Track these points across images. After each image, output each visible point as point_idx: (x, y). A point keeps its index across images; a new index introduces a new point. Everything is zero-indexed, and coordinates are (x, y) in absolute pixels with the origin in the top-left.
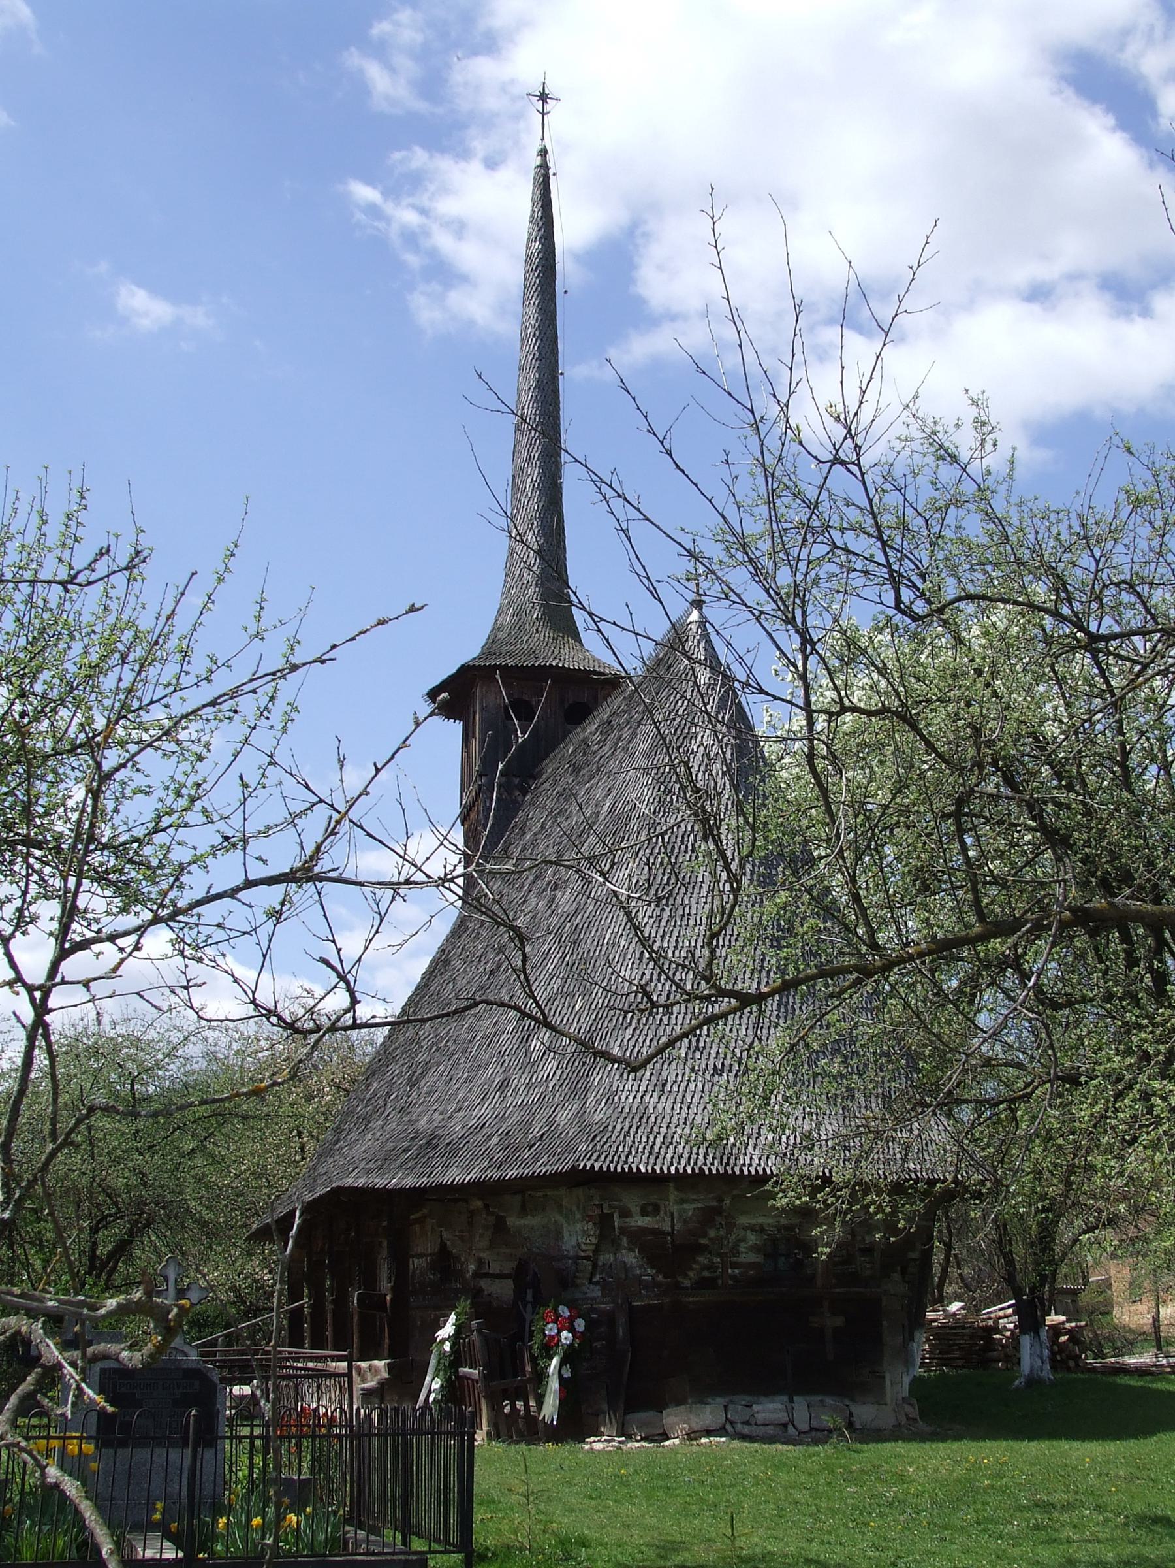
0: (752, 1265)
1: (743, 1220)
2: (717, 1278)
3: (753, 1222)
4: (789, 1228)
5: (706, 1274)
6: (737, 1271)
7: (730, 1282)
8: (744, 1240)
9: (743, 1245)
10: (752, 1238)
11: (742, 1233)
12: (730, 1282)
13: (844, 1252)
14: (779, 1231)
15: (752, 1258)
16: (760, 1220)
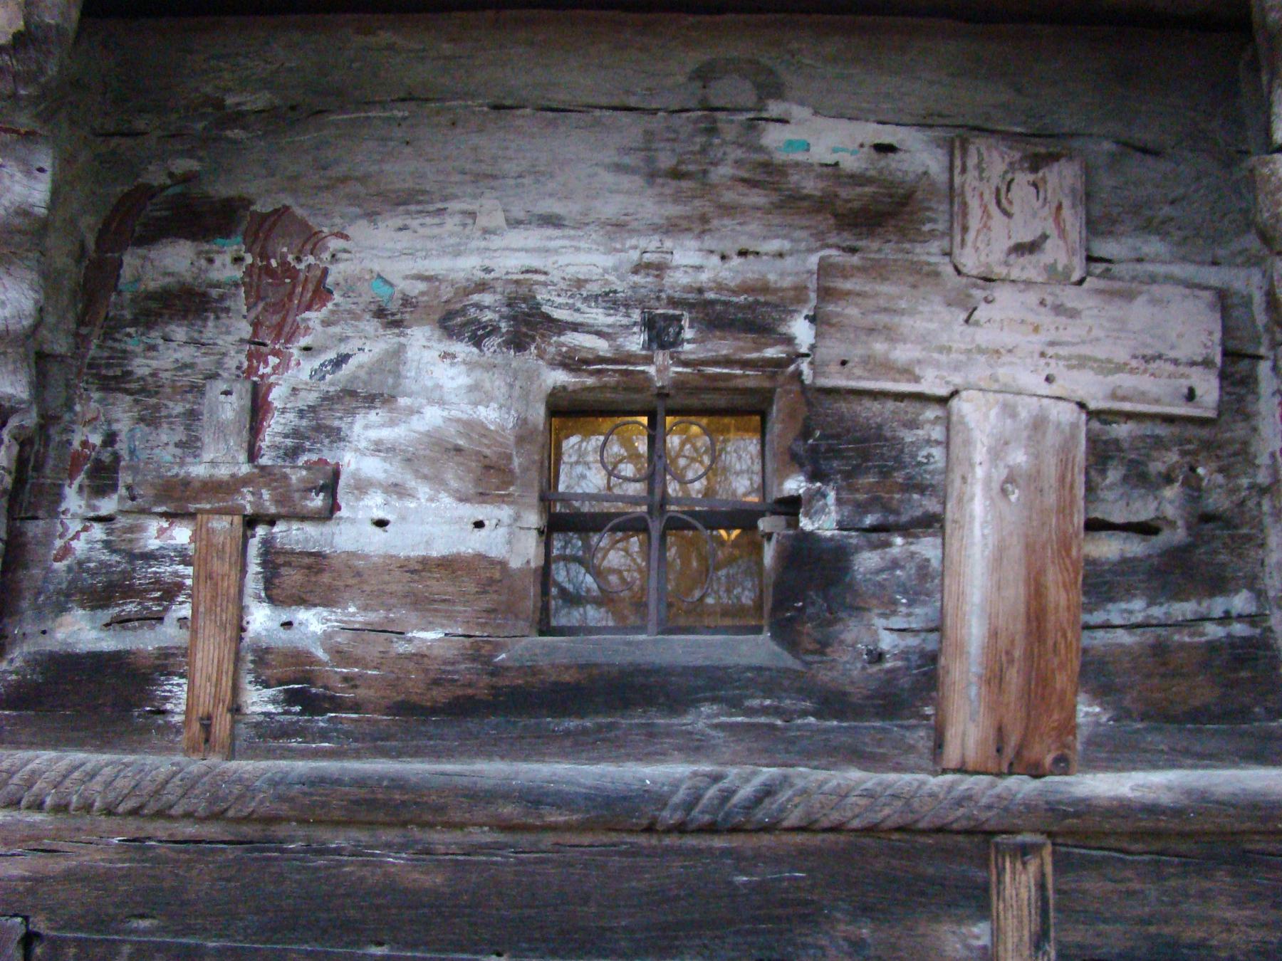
0: (430, 580)
1: (379, 253)
2: (167, 663)
3: (467, 266)
4: (750, 316)
5: (81, 631)
6: (313, 623)
7: (258, 701)
8: (373, 395)
9: (367, 428)
10: (449, 387)
11: (368, 348)
12: (258, 701)
13: (1169, 502)
14: (660, 332)
15: (438, 523)
16: (511, 254)
